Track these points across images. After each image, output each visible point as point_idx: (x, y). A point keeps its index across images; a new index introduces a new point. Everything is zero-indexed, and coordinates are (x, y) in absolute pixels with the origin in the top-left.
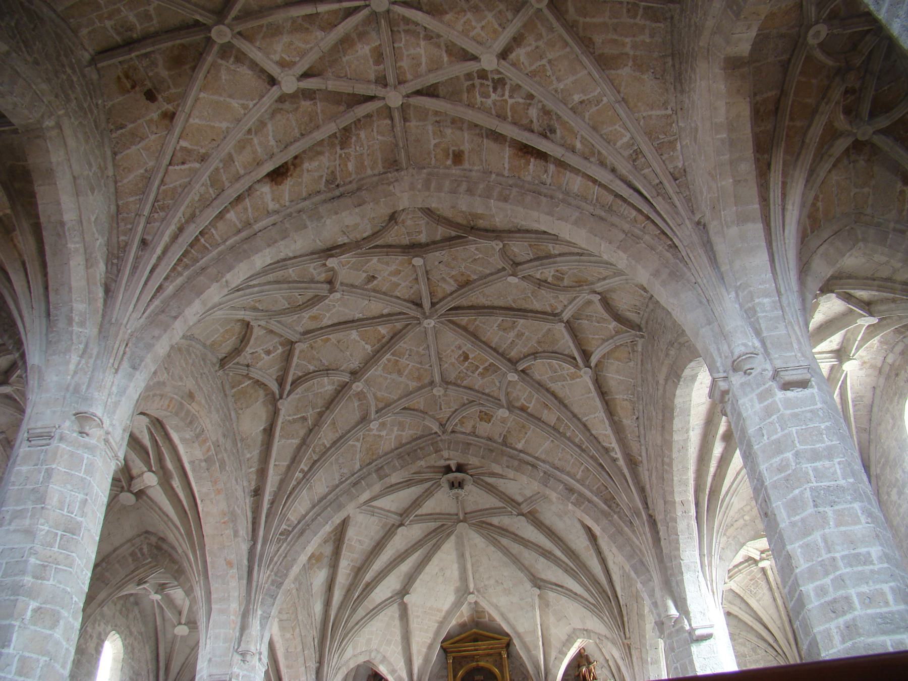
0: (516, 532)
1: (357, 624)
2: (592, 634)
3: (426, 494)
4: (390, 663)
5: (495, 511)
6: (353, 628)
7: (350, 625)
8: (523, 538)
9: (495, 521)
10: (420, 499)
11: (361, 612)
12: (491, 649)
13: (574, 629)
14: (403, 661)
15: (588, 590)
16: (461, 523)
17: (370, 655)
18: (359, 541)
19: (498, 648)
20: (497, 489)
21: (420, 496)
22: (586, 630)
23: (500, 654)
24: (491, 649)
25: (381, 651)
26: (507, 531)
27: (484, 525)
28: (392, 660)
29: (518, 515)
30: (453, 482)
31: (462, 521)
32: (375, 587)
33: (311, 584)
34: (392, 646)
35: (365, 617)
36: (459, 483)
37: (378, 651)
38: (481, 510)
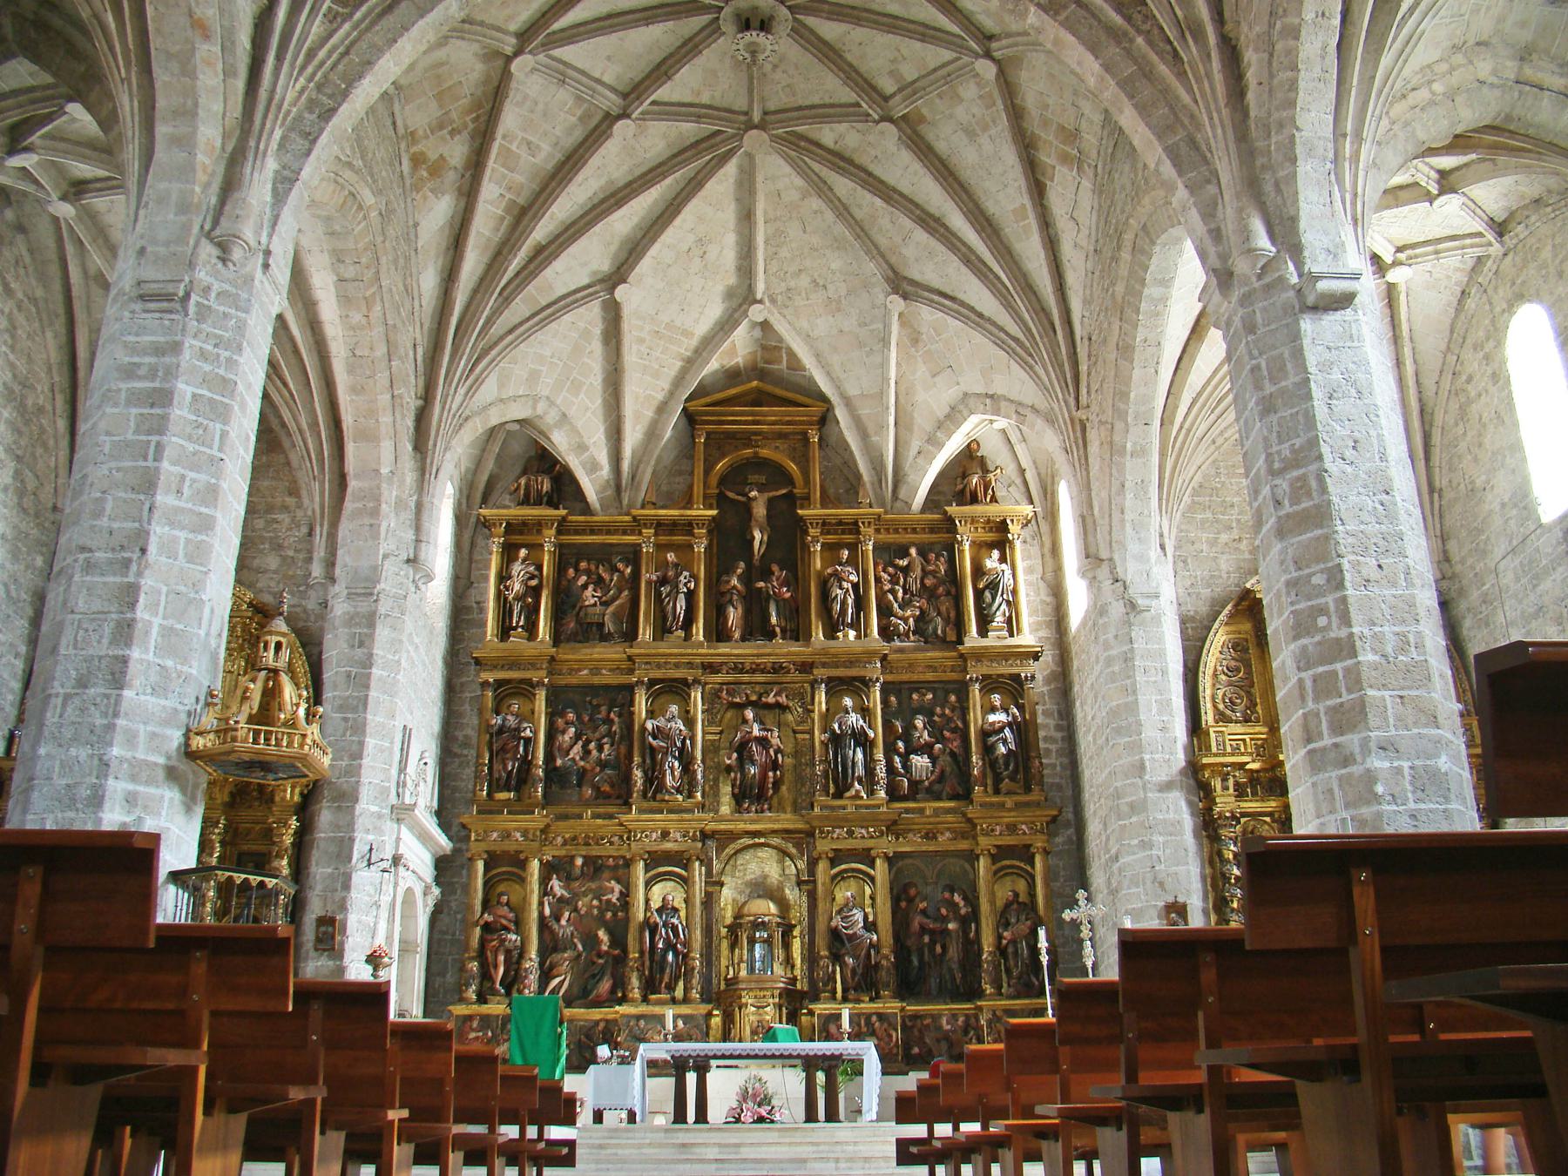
0: (872, 168)
1: (510, 331)
2: (1003, 404)
3: (683, 51)
4: (574, 430)
5: (831, 111)
6: (501, 338)
7: (496, 330)
8: (882, 182)
9: (828, 135)
10: (670, 62)
11: (519, 308)
12: (789, 423)
13: (966, 394)
14: (602, 429)
15: (1009, 306)
16: (754, 132)
17: (534, 408)
18: (529, 143)
19: (801, 423)
20: (841, 56)
21: (671, 55)
22: (992, 397)
23: (805, 435)
24: (789, 423)
25: (558, 402)
26: (851, 162)
27: (803, 144)
28: (579, 424)
29: (883, 119)
30: (748, 20)
31: (756, 127)
32: (555, 255)
33: (416, 225)
34: (582, 395)
35: (528, 319)
36: (762, 22)
37: (552, 403)
38: (800, 108)
